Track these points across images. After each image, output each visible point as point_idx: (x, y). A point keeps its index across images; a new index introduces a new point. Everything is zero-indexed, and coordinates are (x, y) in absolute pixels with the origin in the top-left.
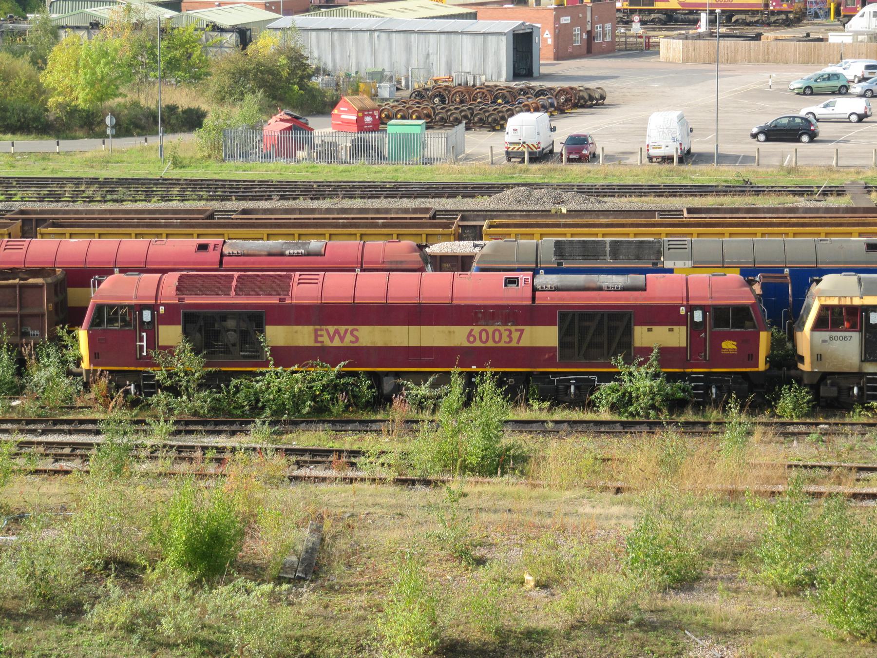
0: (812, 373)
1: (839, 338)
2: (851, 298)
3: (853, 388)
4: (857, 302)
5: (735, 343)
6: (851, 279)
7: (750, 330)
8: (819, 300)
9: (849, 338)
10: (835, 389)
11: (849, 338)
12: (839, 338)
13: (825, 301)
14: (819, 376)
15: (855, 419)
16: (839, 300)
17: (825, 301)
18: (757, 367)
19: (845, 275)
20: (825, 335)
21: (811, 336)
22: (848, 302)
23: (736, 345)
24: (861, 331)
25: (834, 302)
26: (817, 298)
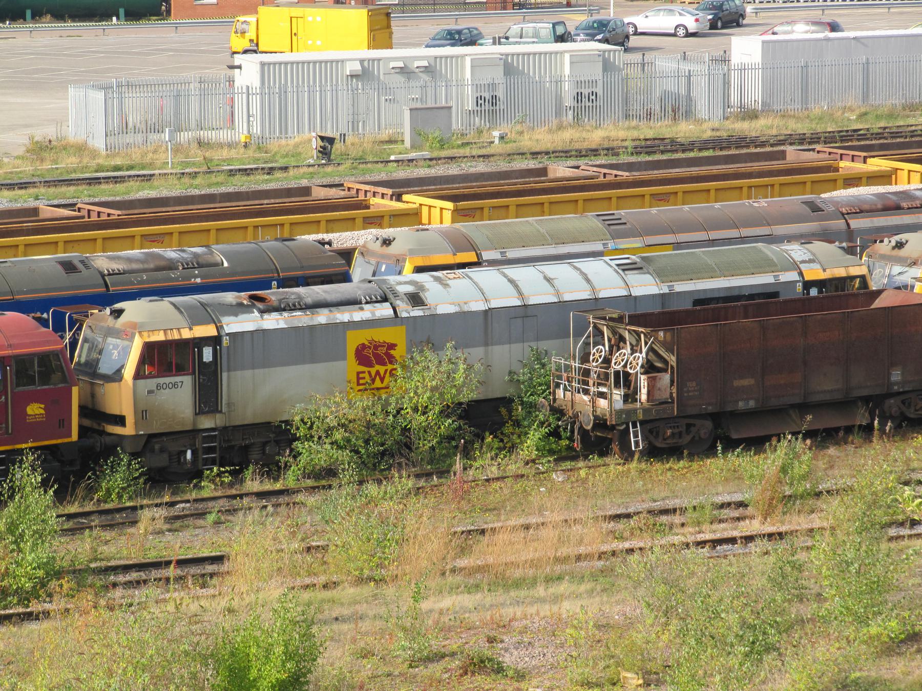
0: (137, 436)
1: (168, 386)
2: (178, 329)
3: (185, 452)
4: (186, 334)
5: (43, 406)
6: (164, 305)
7: (60, 386)
8: (141, 335)
9: (180, 384)
10: (165, 456)
11: (180, 384)
12: (168, 386)
13: (149, 336)
14: (145, 439)
15: (187, 497)
16: (165, 334)
17: (149, 336)
18: (70, 435)
19: (151, 301)
20: (151, 383)
21: (134, 385)
22: (176, 336)
23: (44, 409)
24: (193, 373)
25: (160, 337)
26: (137, 336)
